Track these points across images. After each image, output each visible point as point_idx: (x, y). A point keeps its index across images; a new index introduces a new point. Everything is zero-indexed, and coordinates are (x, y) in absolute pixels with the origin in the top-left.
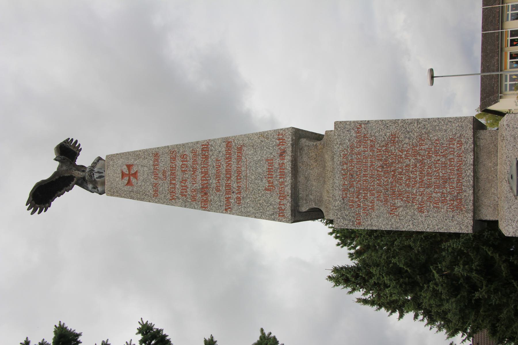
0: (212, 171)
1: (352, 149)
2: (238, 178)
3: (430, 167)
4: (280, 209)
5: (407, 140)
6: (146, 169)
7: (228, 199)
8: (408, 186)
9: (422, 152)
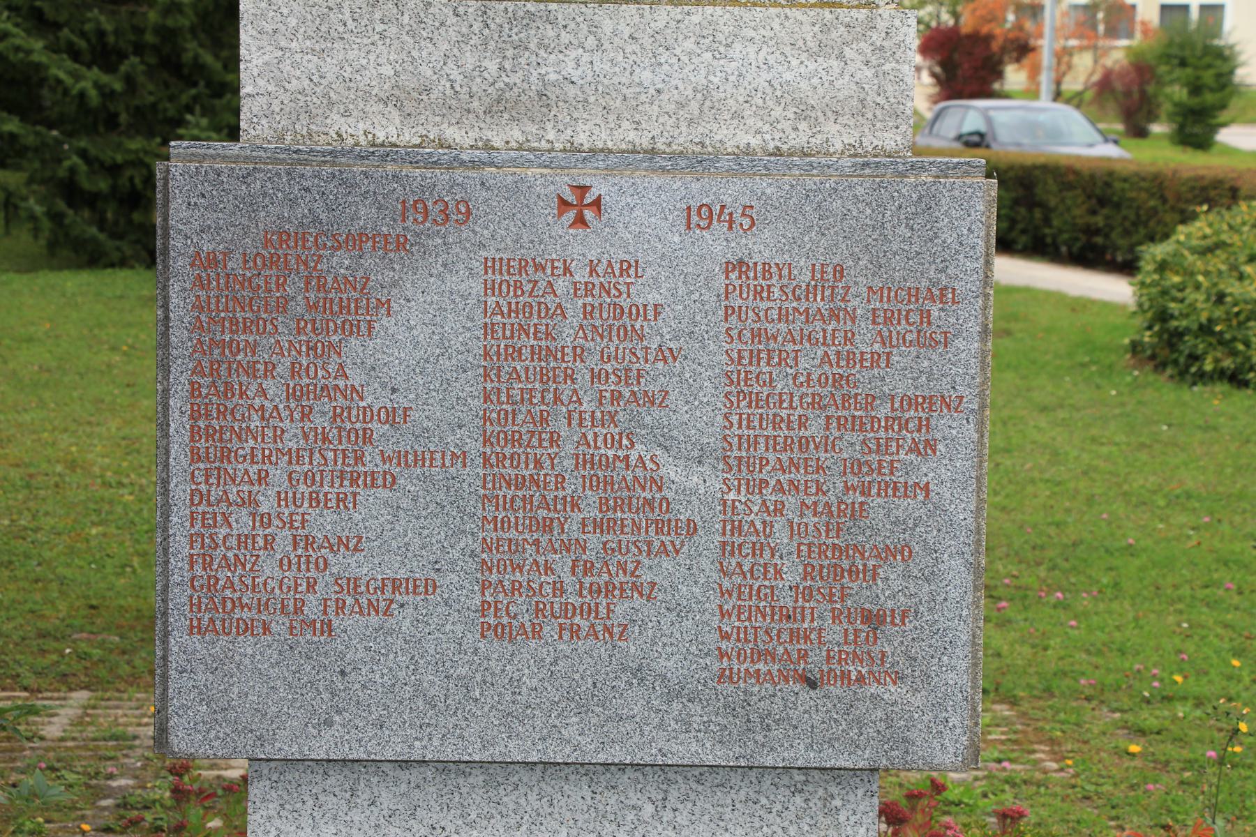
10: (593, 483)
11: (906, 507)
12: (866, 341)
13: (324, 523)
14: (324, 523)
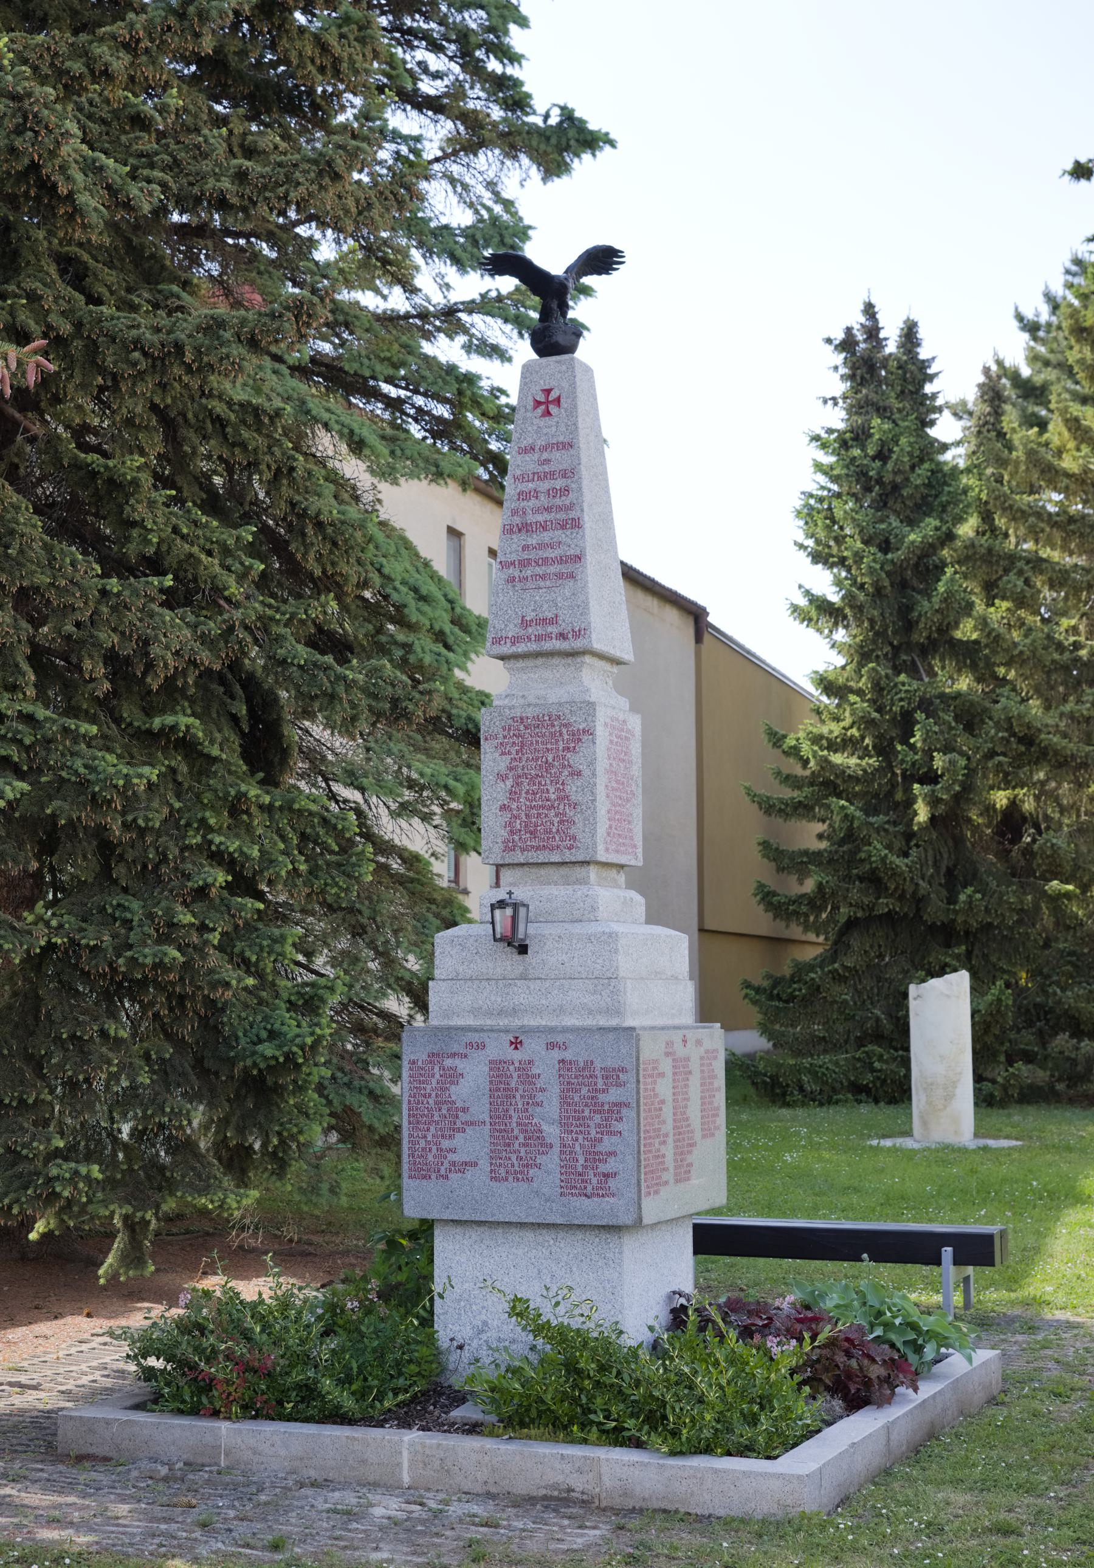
0: (546, 537)
1: (565, 725)
7: (513, 563)
8: (527, 793)
10: (522, 1131)
11: (615, 1139)
13: (446, 1144)
14: (446, 1144)
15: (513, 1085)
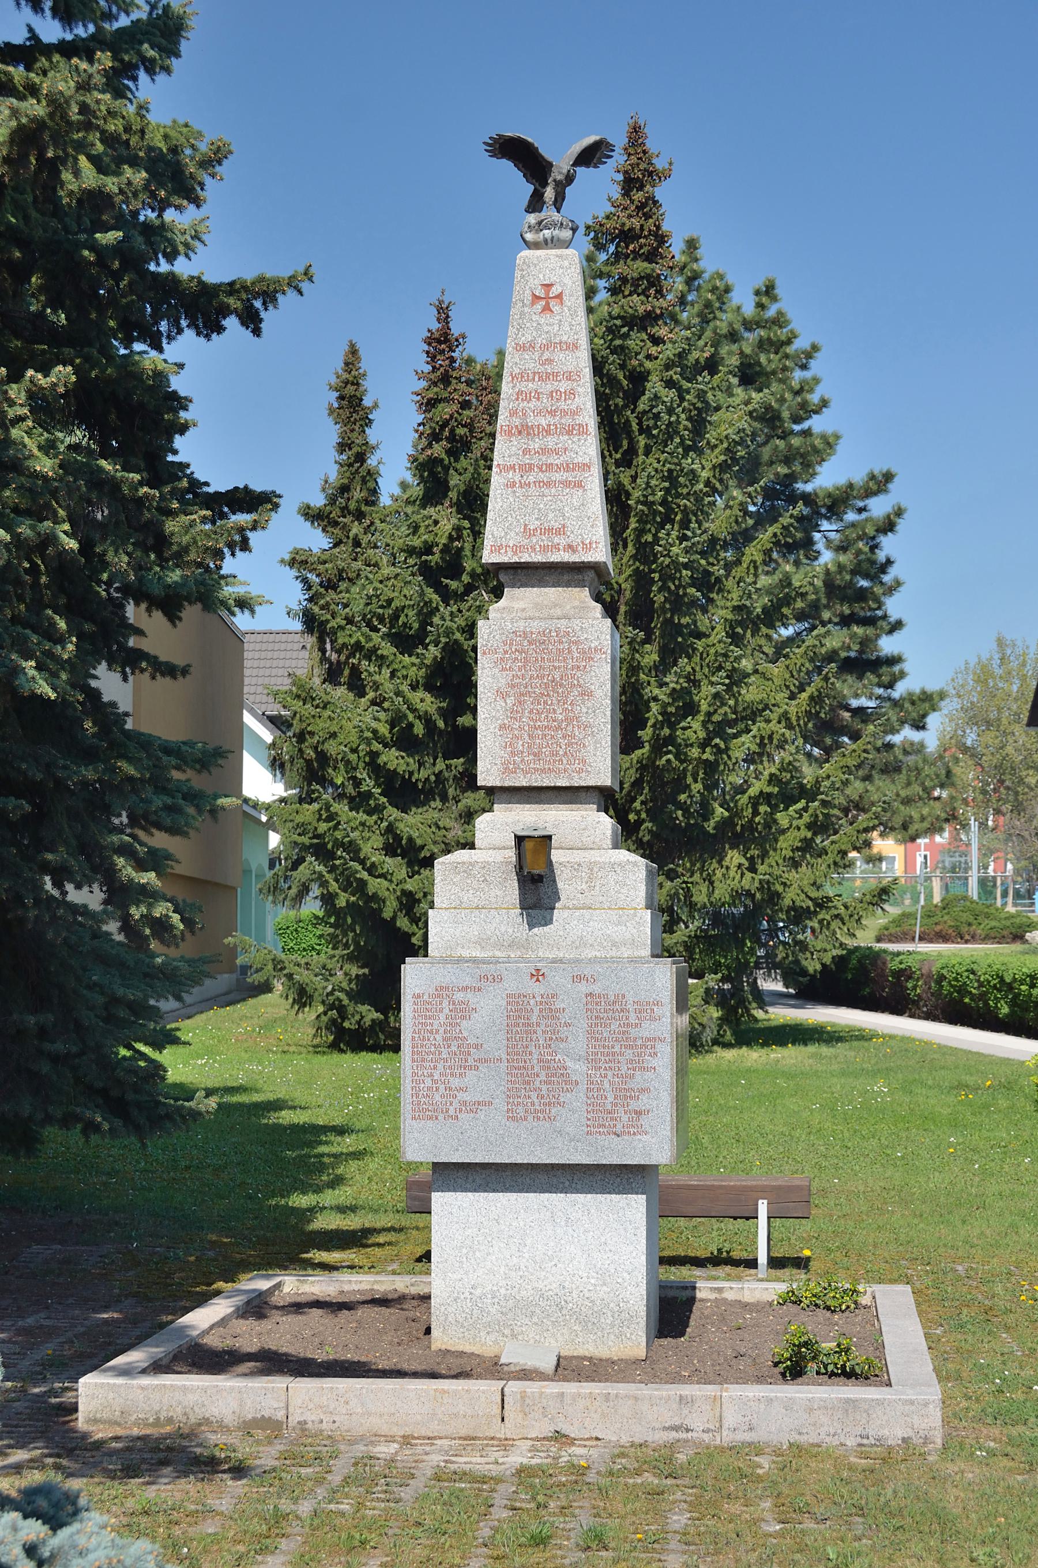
0: (551, 441)
1: (576, 643)
2: (539, 483)
3: (552, 737)
4: (500, 547)
5: (584, 710)
6: (556, 328)
7: (513, 467)
8: (531, 711)
9: (570, 728)
10: (543, 1068)
11: (649, 1075)
12: (633, 1020)
13: (455, 1082)
14: (455, 1082)
15: (534, 1019)
